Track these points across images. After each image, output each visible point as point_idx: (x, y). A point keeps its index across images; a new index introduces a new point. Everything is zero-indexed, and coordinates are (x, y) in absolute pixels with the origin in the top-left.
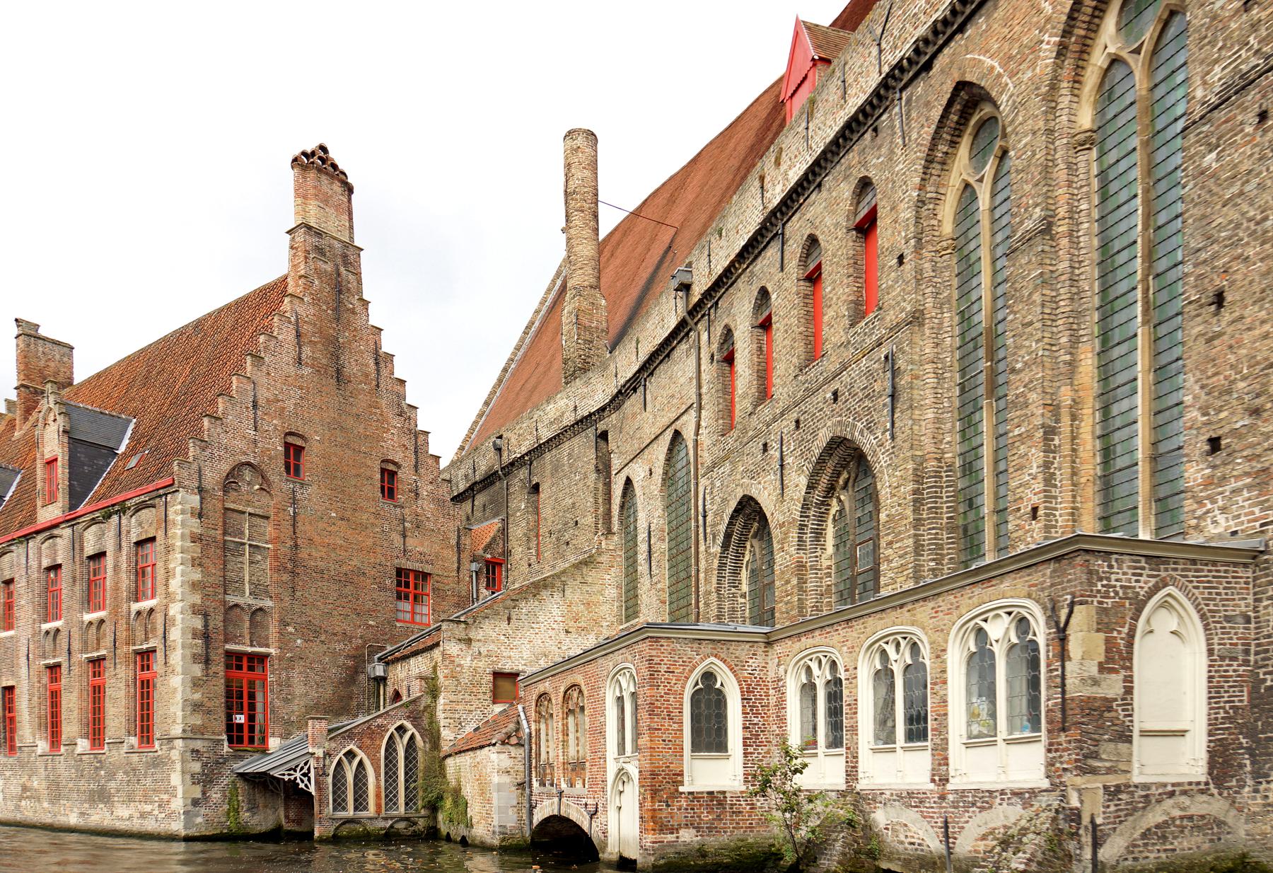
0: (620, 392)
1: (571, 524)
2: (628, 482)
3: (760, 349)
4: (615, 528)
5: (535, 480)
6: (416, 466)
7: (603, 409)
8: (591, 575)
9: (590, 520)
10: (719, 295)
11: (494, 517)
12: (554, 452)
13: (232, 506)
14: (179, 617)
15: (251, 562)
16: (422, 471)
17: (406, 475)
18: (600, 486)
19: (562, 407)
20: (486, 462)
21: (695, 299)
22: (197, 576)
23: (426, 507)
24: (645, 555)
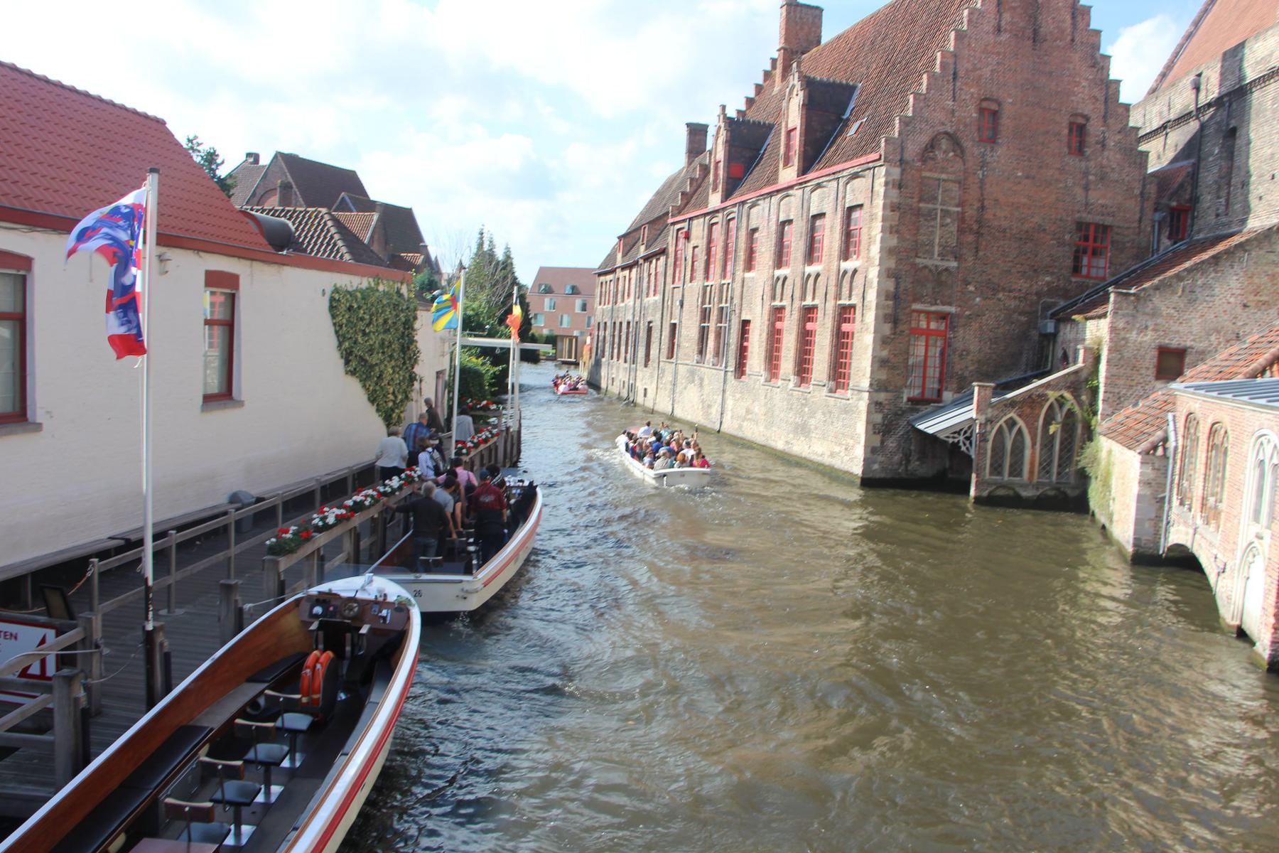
6: (1105, 117)
13: (925, 174)
14: (876, 281)
15: (942, 226)
16: (1111, 121)
17: (1095, 128)
22: (894, 242)
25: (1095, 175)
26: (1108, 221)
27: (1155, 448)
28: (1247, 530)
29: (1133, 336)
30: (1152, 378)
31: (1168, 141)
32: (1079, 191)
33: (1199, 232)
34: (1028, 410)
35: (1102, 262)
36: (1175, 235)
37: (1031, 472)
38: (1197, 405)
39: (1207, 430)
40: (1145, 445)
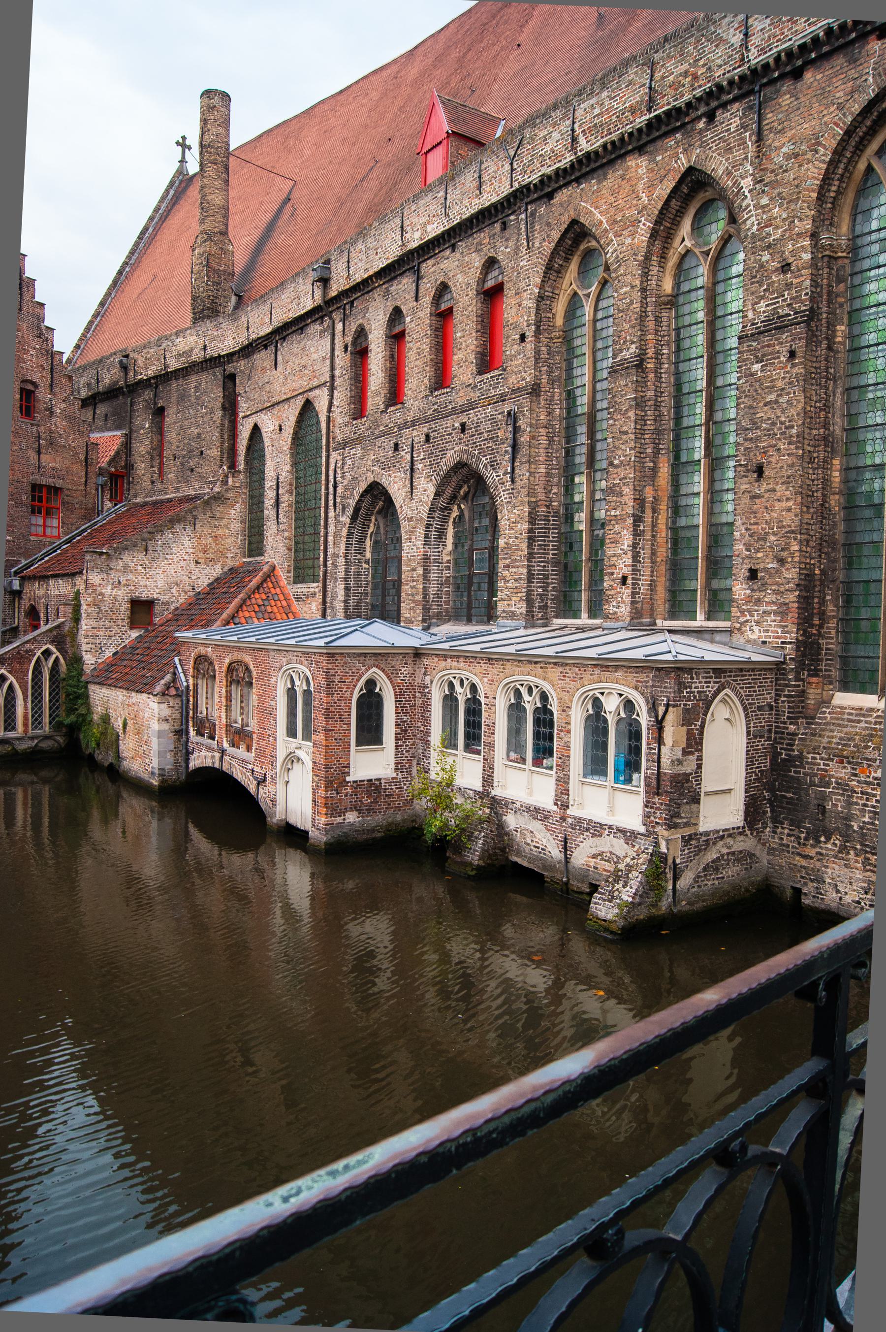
0: (250, 344)
1: (197, 452)
2: (256, 429)
3: (392, 356)
4: (241, 467)
5: (161, 403)
6: (51, 385)
7: (231, 355)
8: (219, 509)
9: (215, 452)
10: (355, 296)
11: (117, 428)
12: (181, 381)
16: (56, 390)
17: (43, 394)
18: (226, 423)
19: (191, 343)
20: (110, 377)
21: (333, 293)
23: (59, 424)
24: (272, 502)
25: (46, 440)
26: (59, 483)
27: (168, 688)
28: (283, 745)
29: (108, 590)
30: (126, 628)
31: (98, 412)
32: (32, 455)
33: (135, 496)
34: (18, 666)
35: (55, 523)
36: (116, 498)
37: (25, 725)
38: (209, 650)
39: (224, 669)
40: (158, 688)
